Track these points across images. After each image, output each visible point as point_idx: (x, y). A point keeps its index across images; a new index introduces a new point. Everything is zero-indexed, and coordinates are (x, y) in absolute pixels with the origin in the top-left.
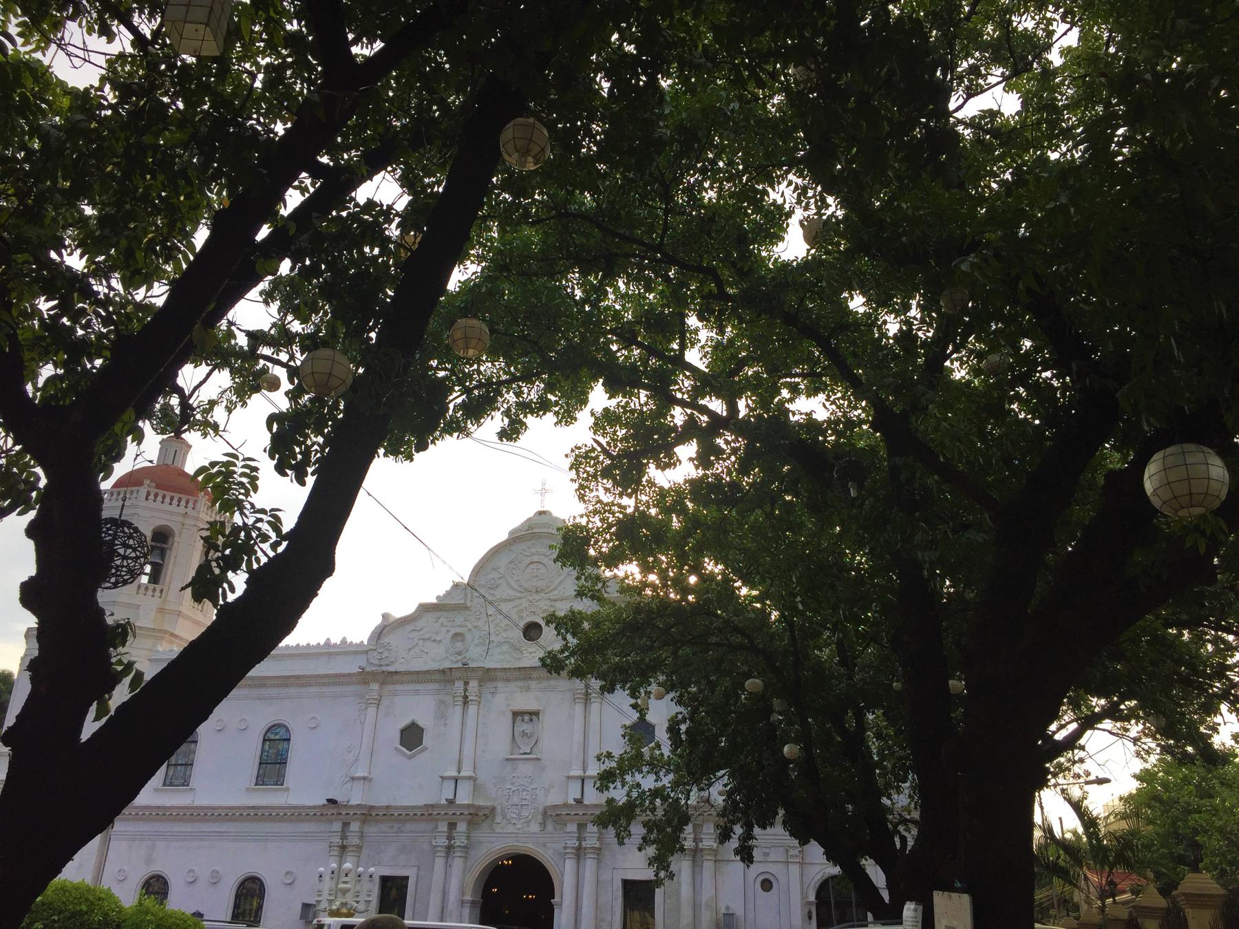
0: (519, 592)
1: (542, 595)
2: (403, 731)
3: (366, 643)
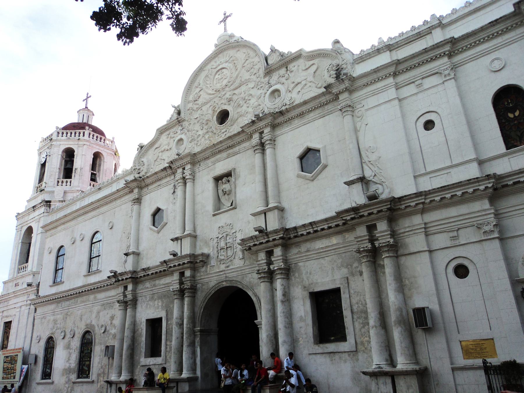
0: (213, 94)
1: (227, 89)
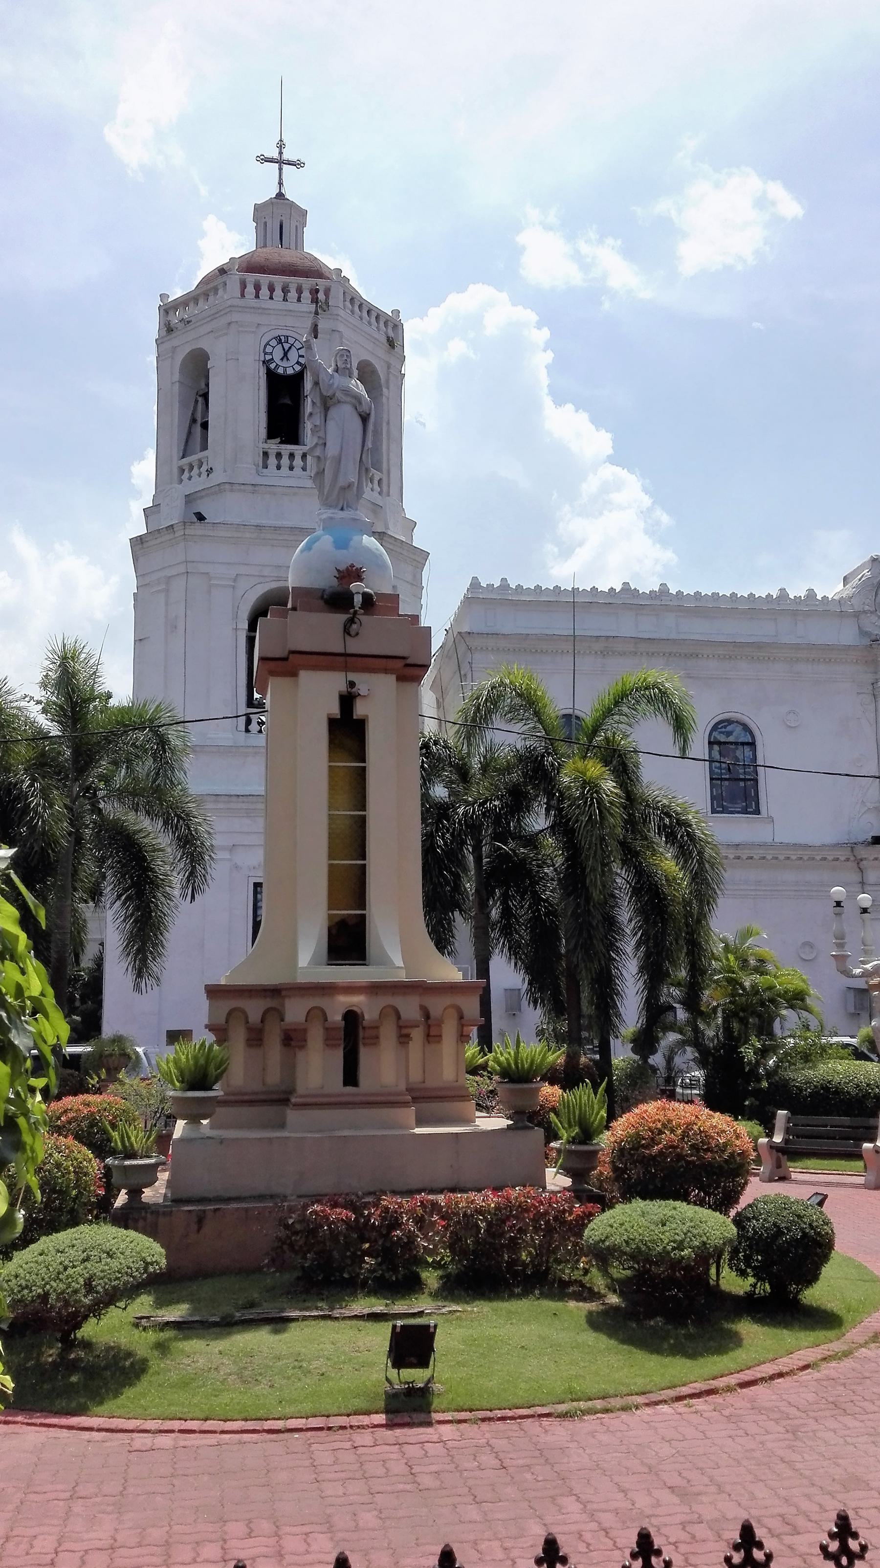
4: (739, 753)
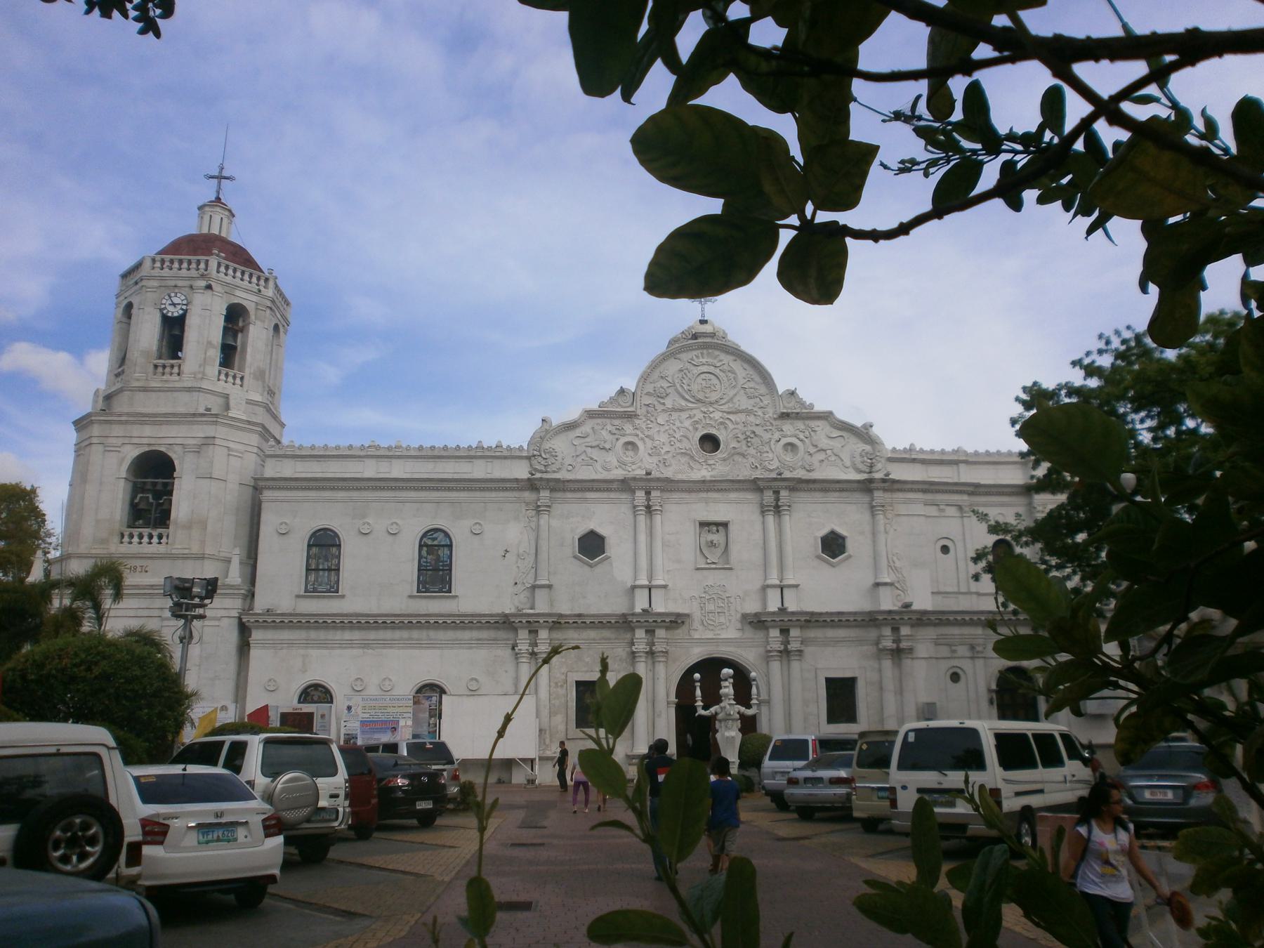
1: (715, 406)
2: (583, 540)
3: (526, 448)
4: (440, 552)
